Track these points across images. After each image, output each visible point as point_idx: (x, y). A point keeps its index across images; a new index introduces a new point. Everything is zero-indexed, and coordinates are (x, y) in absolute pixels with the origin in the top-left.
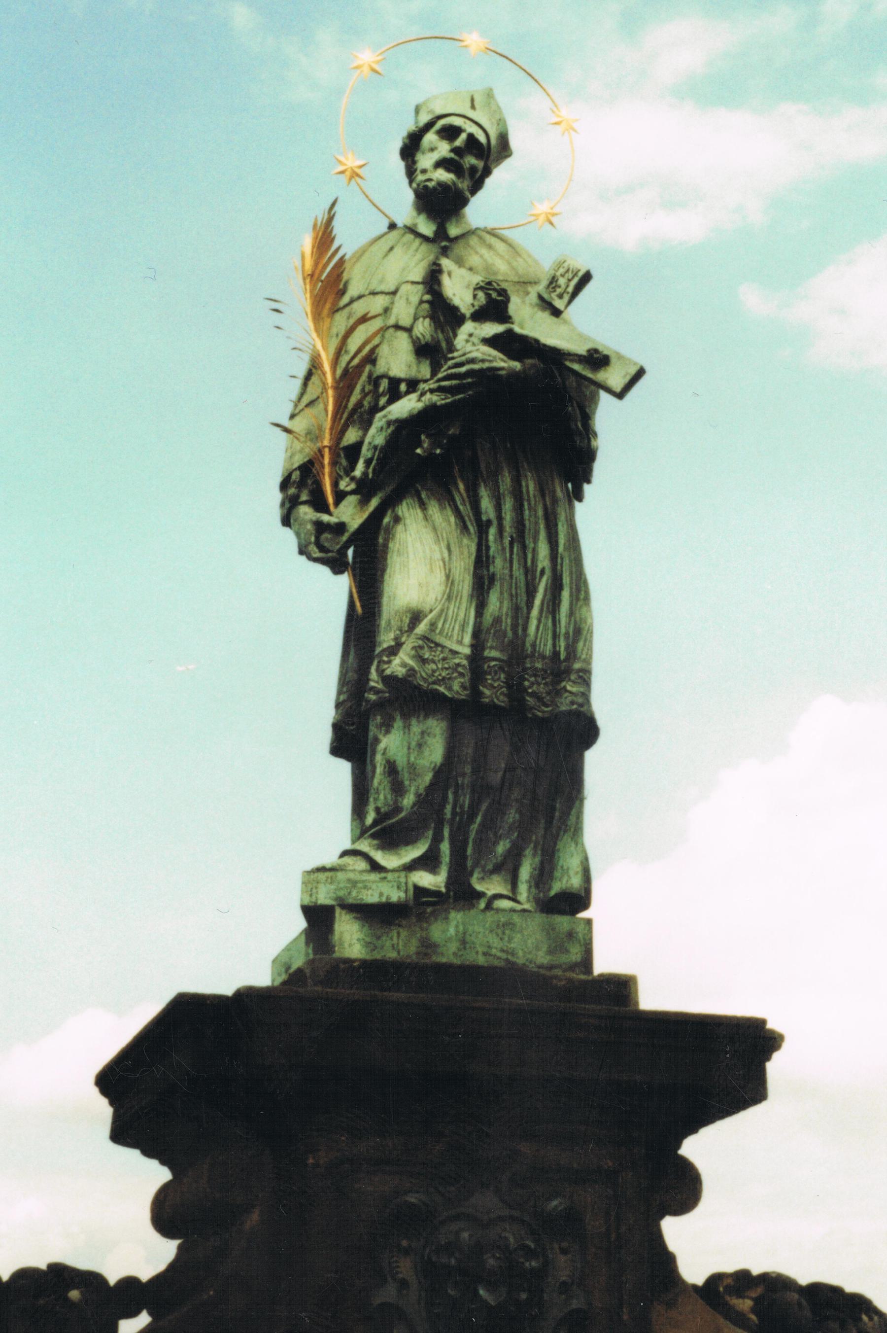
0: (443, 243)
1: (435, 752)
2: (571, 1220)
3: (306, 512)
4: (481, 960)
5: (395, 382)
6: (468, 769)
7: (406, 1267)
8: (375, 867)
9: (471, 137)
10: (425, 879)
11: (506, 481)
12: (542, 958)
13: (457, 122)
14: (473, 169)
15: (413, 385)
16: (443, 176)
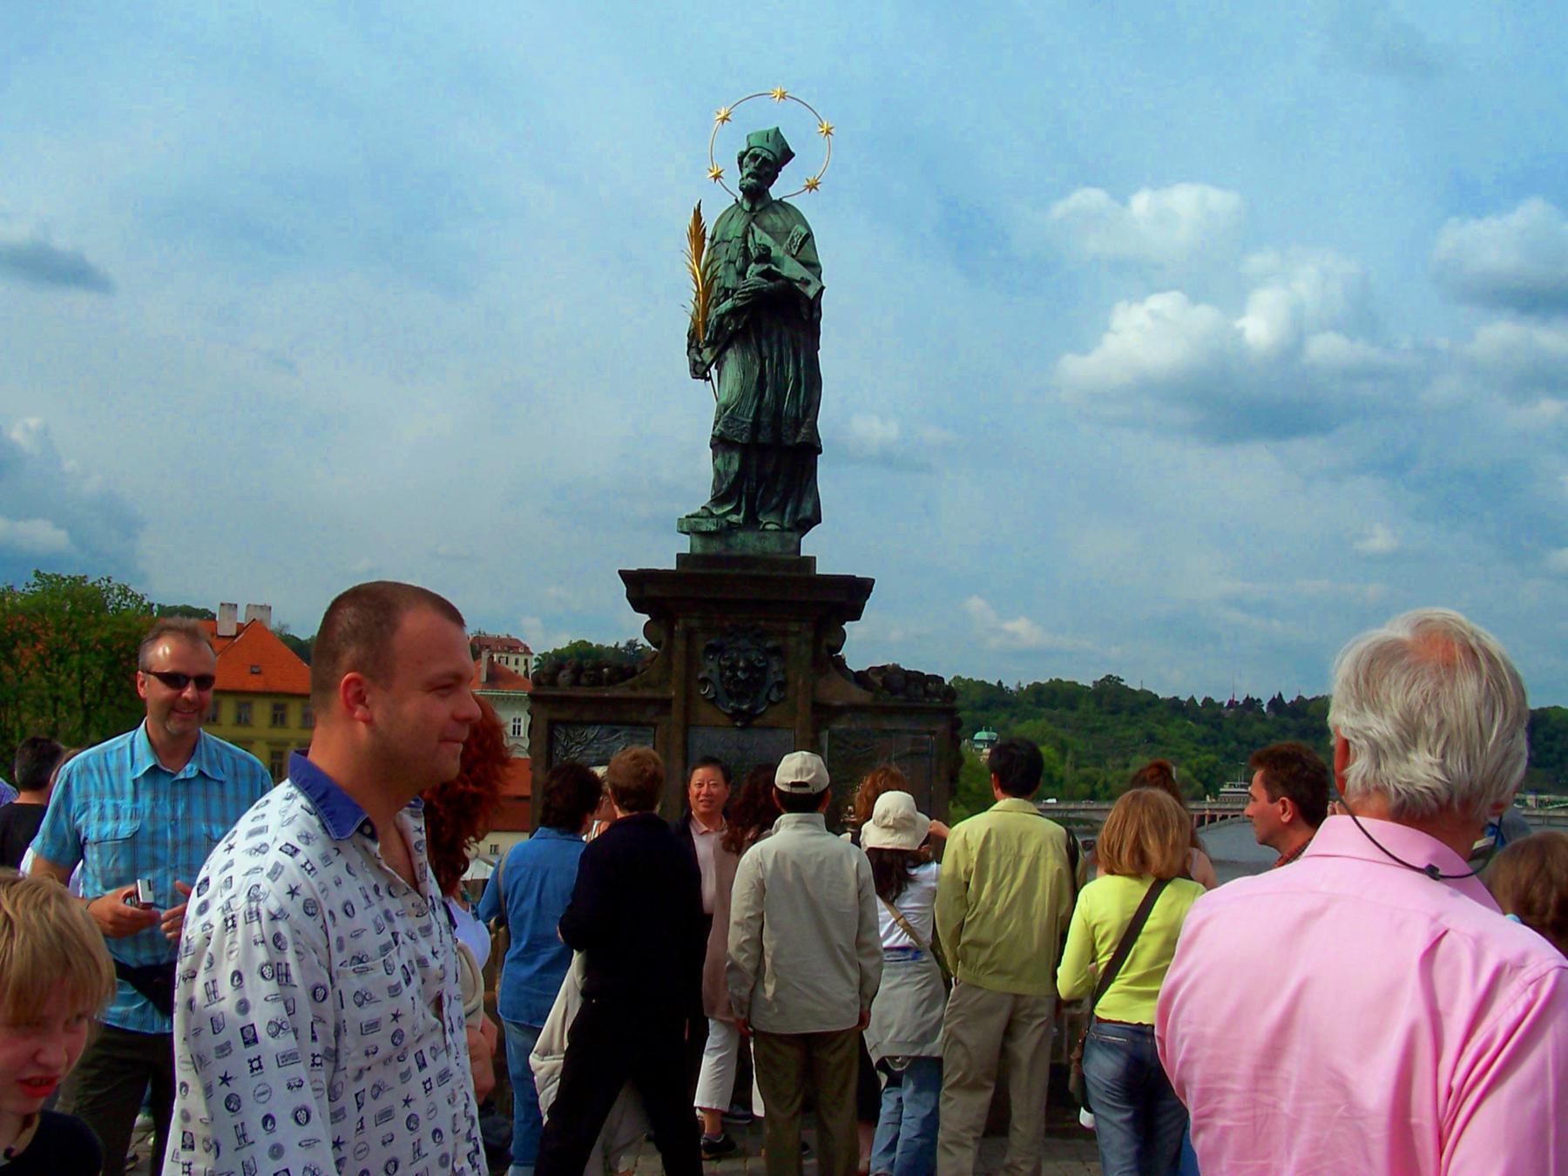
0: (754, 216)
1: (735, 465)
2: (776, 651)
3: (693, 351)
4: (751, 552)
5: (727, 290)
6: (754, 469)
7: (713, 666)
8: (712, 515)
9: (764, 159)
10: (734, 518)
11: (774, 338)
12: (778, 549)
13: (758, 151)
14: (767, 174)
15: (734, 291)
16: (751, 181)
